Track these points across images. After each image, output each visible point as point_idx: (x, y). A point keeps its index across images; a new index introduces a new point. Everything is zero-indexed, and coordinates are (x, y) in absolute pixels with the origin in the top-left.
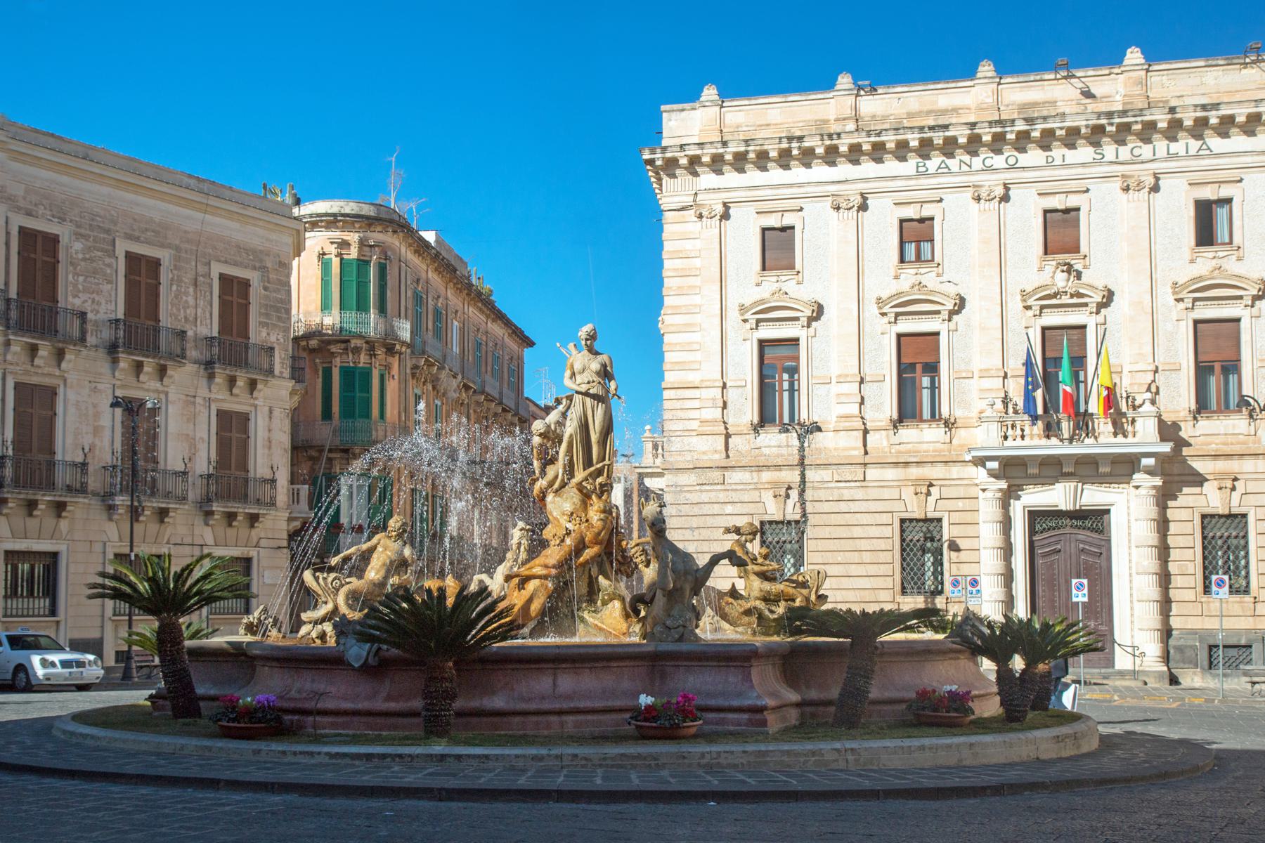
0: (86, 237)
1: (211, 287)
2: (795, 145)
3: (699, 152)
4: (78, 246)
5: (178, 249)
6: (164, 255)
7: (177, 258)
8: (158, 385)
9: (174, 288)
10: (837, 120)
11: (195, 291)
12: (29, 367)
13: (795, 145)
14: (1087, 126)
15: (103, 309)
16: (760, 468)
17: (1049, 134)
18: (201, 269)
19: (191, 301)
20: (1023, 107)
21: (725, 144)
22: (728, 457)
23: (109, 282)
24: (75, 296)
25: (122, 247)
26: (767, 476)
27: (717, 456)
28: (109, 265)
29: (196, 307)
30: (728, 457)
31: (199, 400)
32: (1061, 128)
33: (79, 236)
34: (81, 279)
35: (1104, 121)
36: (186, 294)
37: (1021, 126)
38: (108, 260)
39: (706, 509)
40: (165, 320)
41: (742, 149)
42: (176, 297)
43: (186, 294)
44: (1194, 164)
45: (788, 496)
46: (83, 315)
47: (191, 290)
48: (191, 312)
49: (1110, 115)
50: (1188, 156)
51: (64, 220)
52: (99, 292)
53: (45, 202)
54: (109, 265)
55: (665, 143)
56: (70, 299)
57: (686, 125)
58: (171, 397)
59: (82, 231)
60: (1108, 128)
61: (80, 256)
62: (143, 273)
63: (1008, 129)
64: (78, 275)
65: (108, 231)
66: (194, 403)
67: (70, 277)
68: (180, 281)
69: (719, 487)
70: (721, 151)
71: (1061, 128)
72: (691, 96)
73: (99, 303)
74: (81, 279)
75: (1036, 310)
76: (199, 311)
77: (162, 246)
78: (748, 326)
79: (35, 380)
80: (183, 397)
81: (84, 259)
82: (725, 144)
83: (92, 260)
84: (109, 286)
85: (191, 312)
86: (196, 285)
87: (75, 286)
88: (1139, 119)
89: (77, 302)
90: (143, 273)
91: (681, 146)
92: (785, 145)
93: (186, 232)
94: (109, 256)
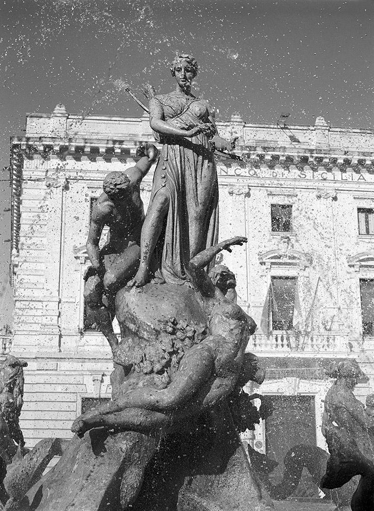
2: (117, 146)
3: (52, 143)
10: (143, 135)
13: (117, 146)
14: (298, 156)
16: (83, 360)
17: (275, 158)
20: (258, 141)
21: (70, 140)
22: (60, 351)
26: (89, 365)
27: (53, 350)
30: (60, 351)
32: (283, 156)
35: (308, 155)
37: (260, 151)
39: (42, 388)
41: (82, 144)
44: (355, 186)
45: (102, 381)
49: (311, 151)
50: (353, 182)
55: (28, 135)
57: (44, 127)
60: (311, 159)
63: (252, 152)
69: (54, 372)
70: (67, 144)
71: (283, 156)
72: (48, 111)
75: (268, 265)
78: (79, 261)
82: (70, 140)
88: (327, 156)
91: (40, 138)
92: (110, 145)
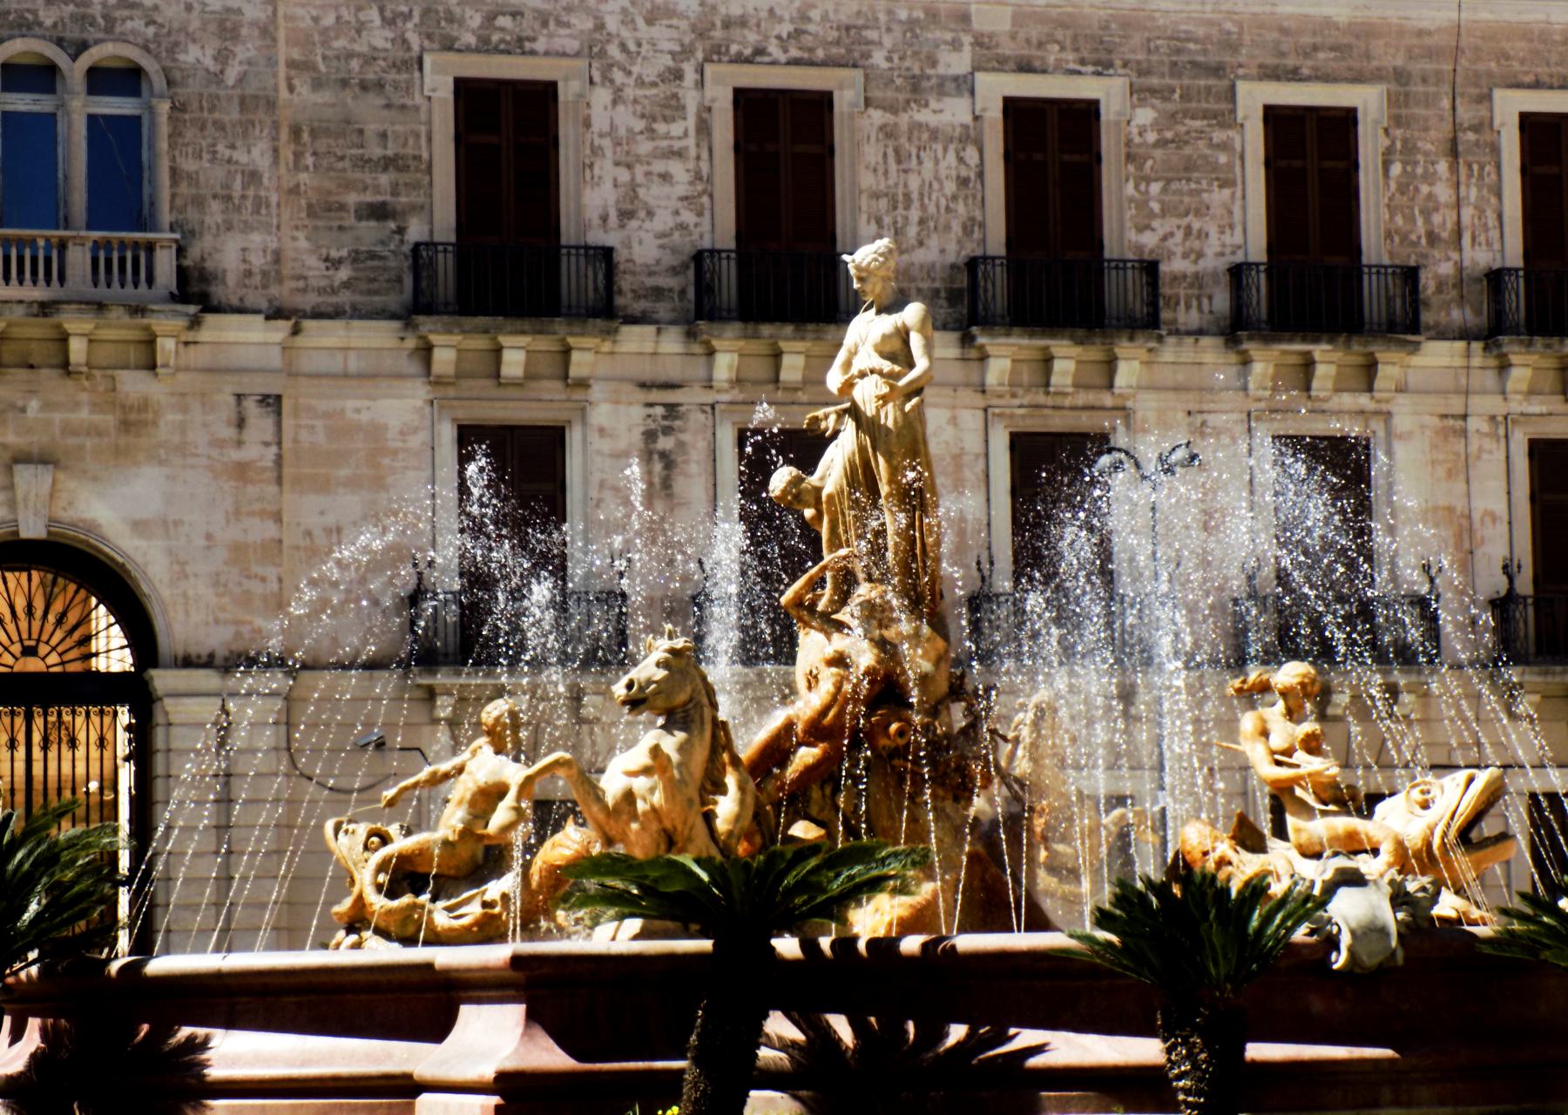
0: (1164, 93)
1: (1495, 149)
4: (1145, 116)
5: (1401, 76)
6: (1366, 99)
7: (1398, 102)
8: (1364, 400)
9: (1396, 169)
11: (1454, 169)
12: (1041, 399)
15: (1213, 245)
18: (1466, 114)
19: (1443, 193)
23: (1225, 183)
24: (1141, 229)
25: (1254, 97)
28: (1225, 146)
29: (1458, 206)
31: (1473, 424)
33: (1140, 93)
34: (1155, 188)
36: (1430, 178)
38: (1218, 136)
40: (1374, 245)
42: (1402, 189)
43: (1430, 178)
46: (1150, 269)
47: (1442, 167)
48: (1443, 220)
51: (1110, 65)
52: (1201, 211)
53: (1059, 34)
54: (1225, 146)
56: (1132, 235)
58: (1402, 422)
59: (1155, 81)
61: (1151, 137)
62: (1312, 157)
64: (1148, 180)
65: (1217, 70)
66: (1464, 433)
67: (1130, 189)
68: (1409, 149)
73: (1203, 235)
74: (1155, 188)
76: (1467, 214)
77: (1358, 78)
79: (1058, 423)
80: (1436, 421)
81: (1162, 143)
83: (1180, 142)
84: (1227, 192)
85: (1443, 220)
86: (1454, 152)
87: (1142, 205)
89: (1149, 240)
90: (1312, 157)
93: (1421, 33)
94: (1223, 125)
